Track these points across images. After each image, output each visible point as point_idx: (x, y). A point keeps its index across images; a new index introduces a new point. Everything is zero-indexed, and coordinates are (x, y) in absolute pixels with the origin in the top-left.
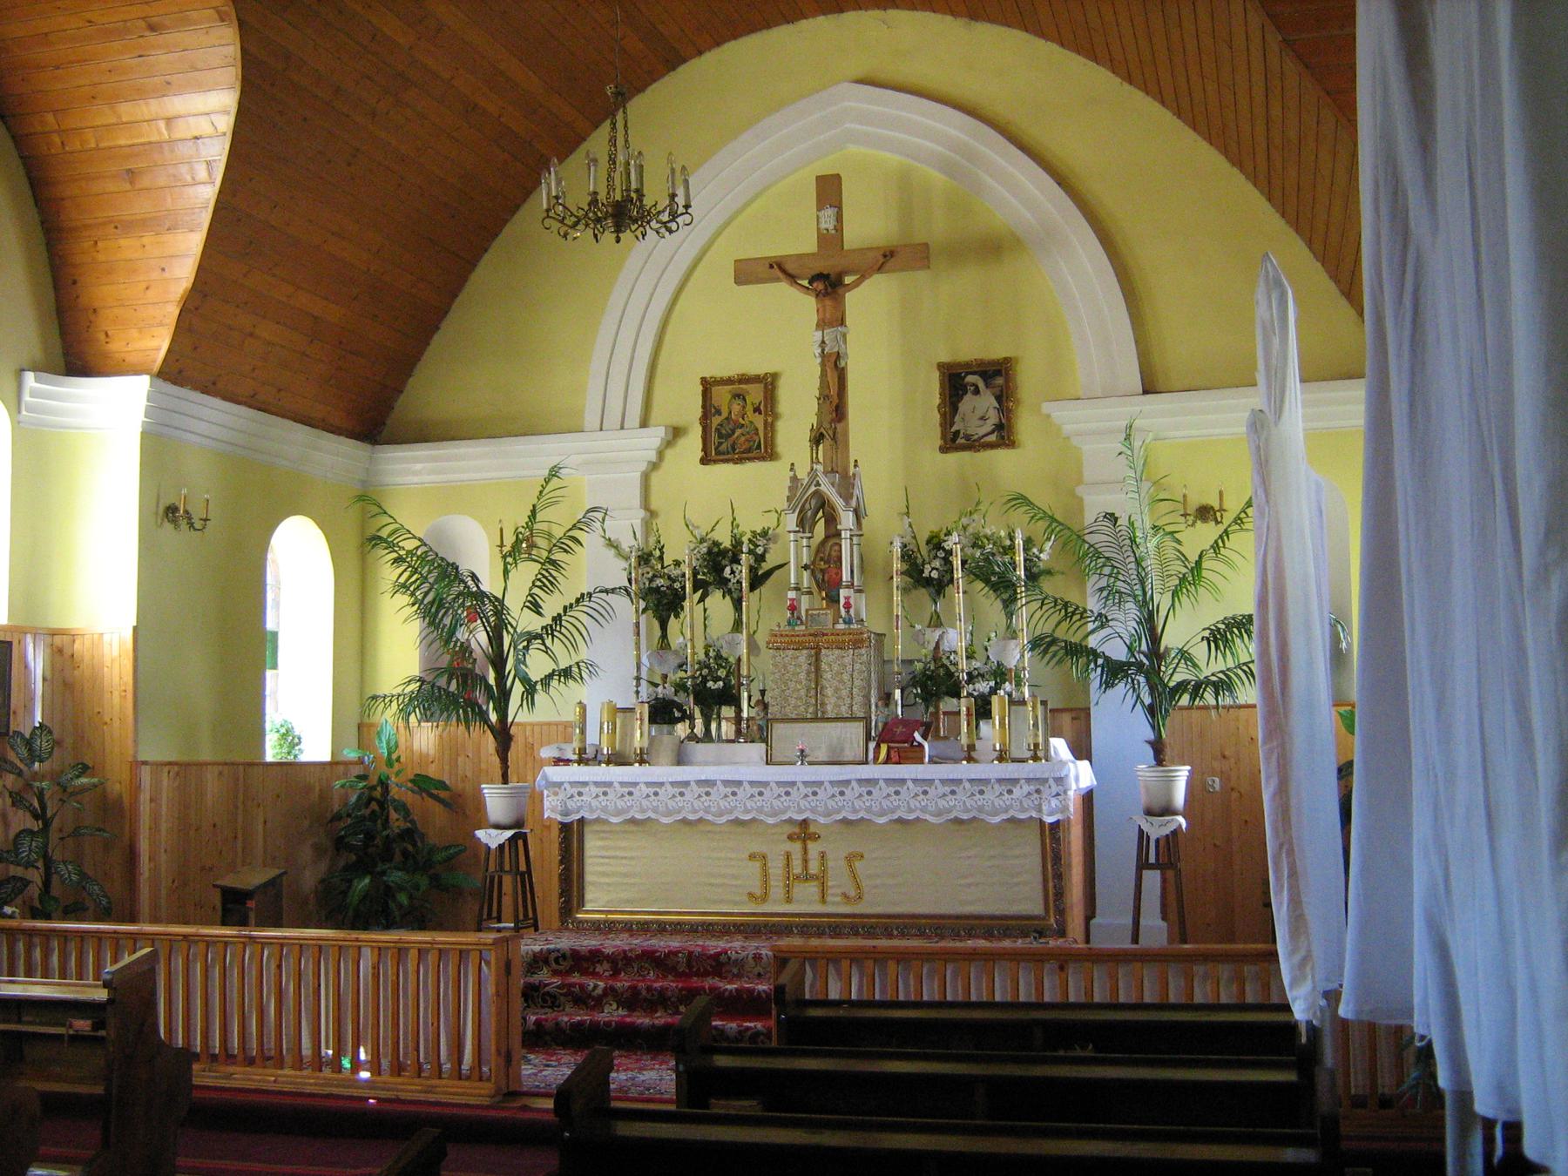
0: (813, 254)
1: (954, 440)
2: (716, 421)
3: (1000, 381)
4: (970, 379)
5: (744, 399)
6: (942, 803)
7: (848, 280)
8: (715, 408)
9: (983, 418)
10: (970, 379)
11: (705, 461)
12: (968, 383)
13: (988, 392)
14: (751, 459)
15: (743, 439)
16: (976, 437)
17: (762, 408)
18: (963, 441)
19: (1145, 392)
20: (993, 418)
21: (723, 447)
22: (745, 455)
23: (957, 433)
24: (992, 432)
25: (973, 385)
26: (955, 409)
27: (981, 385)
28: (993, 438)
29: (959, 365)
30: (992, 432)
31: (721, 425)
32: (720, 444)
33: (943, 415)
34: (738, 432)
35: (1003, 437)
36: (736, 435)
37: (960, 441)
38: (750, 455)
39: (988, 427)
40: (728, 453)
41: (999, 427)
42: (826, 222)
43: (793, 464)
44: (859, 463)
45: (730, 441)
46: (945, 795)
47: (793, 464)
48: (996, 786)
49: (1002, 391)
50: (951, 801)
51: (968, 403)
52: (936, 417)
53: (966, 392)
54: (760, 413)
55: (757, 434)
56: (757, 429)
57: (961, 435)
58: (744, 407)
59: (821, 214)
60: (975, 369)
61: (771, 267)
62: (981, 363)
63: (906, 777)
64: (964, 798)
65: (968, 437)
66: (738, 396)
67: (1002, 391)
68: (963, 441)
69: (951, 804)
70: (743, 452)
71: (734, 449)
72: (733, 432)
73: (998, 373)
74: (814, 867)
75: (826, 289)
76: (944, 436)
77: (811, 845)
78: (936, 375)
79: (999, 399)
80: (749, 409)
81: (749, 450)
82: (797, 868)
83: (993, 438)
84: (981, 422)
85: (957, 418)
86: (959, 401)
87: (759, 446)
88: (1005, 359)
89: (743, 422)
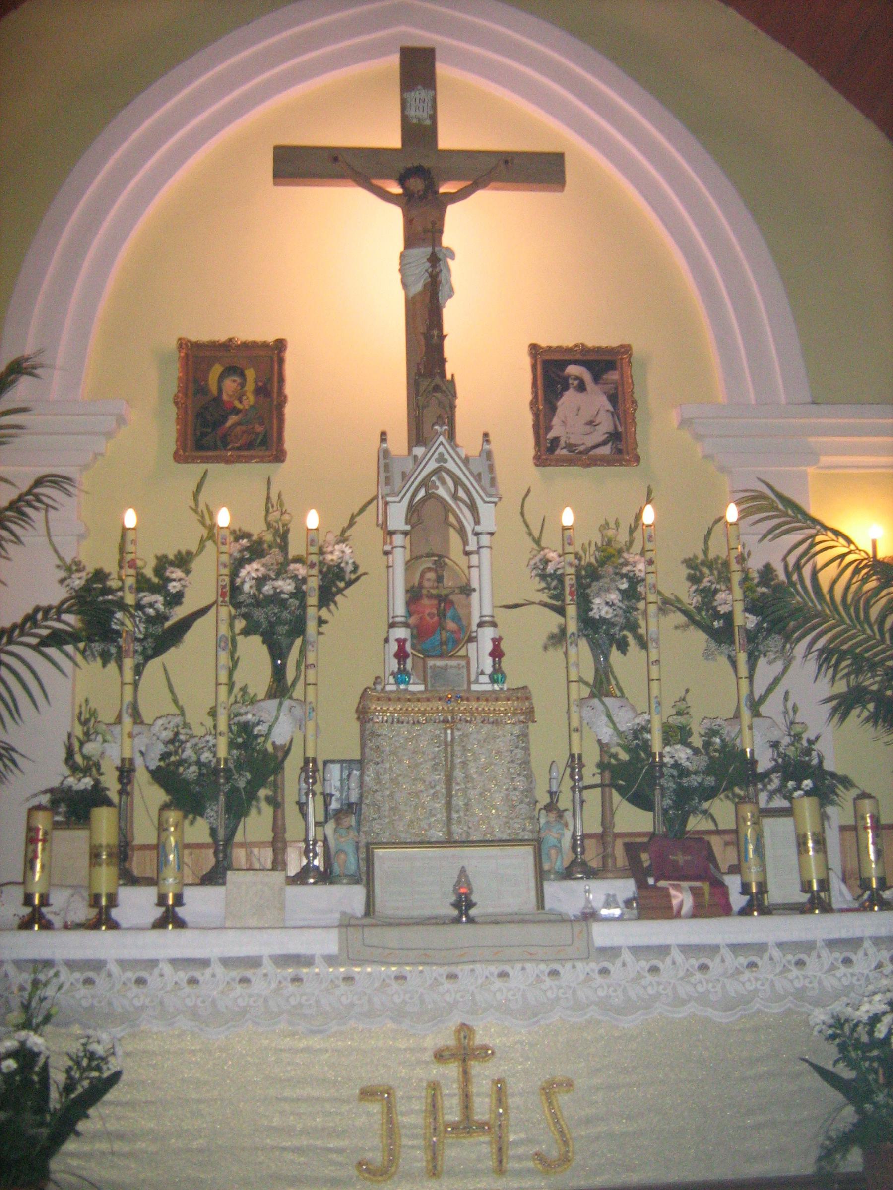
0: (396, 150)
3: (613, 376)
5: (242, 375)
6: (733, 988)
9: (590, 423)
12: (569, 376)
16: (582, 448)
18: (564, 452)
19: (814, 403)
20: (606, 425)
22: (246, 453)
23: (556, 440)
24: (604, 443)
25: (576, 378)
26: (552, 409)
27: (587, 376)
28: (606, 450)
29: (559, 349)
30: (604, 443)
33: (536, 415)
34: (232, 419)
36: (229, 424)
37: (561, 452)
39: (599, 436)
40: (215, 448)
41: (615, 437)
42: (417, 108)
44: (491, 438)
46: (738, 972)
48: (825, 953)
49: (616, 388)
50: (749, 981)
51: (569, 400)
52: (528, 418)
53: (566, 388)
57: (562, 443)
58: (243, 385)
60: (579, 357)
62: (584, 349)
63: (668, 942)
64: (771, 976)
65: (570, 447)
66: (232, 370)
67: (616, 388)
68: (564, 452)
69: (750, 987)
70: (239, 449)
72: (225, 418)
73: (611, 365)
74: (482, 1108)
77: (476, 1068)
78: (526, 361)
79: (613, 398)
80: (250, 386)
81: (249, 446)
82: (452, 1113)
83: (606, 450)
84: (588, 429)
85: (556, 421)
86: (558, 399)
88: (622, 346)
89: (240, 406)
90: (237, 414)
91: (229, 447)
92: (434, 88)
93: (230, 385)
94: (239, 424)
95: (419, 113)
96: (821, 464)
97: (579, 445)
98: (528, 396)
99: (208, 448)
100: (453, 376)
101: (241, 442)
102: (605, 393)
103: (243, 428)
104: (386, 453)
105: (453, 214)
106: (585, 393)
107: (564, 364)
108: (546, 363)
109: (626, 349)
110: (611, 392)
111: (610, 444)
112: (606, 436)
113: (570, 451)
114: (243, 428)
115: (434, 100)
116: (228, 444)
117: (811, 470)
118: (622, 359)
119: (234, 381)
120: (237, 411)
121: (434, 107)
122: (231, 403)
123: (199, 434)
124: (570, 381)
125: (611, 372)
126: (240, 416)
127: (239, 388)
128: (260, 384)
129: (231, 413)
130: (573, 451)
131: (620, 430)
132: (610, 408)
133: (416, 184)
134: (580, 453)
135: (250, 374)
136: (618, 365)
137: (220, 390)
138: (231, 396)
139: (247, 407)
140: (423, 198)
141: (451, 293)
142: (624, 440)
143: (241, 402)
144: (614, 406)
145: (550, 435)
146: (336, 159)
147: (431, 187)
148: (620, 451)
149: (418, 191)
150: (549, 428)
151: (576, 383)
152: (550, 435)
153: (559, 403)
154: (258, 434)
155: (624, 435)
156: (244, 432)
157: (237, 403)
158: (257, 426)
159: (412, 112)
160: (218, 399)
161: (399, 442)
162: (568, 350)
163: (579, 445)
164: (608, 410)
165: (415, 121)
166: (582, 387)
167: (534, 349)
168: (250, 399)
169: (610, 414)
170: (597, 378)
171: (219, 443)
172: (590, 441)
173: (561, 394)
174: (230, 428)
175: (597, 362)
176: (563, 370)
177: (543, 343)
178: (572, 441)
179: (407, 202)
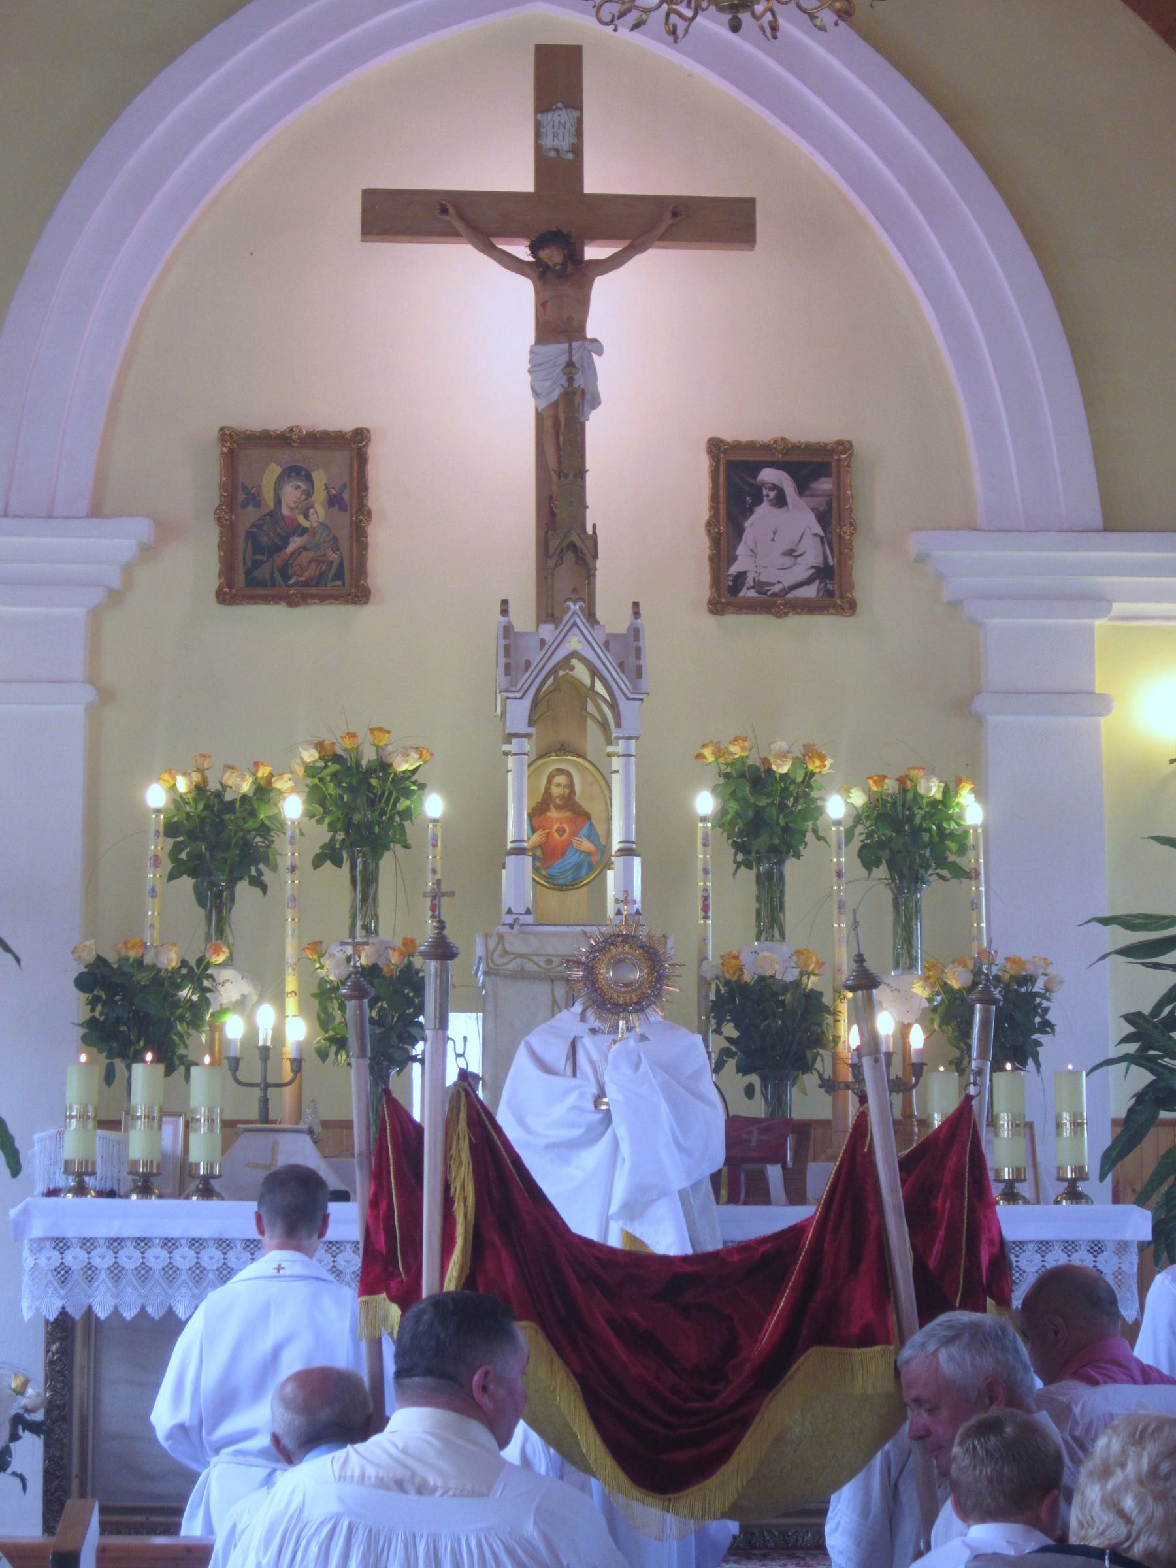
1: (735, 589)
2: (250, 516)
3: (825, 485)
4: (768, 475)
5: (309, 479)
7: (593, 252)
8: (245, 488)
9: (790, 553)
10: (768, 475)
11: (228, 595)
12: (763, 484)
13: (801, 502)
14: (323, 599)
15: (305, 557)
16: (776, 588)
17: (346, 496)
18: (752, 594)
20: (812, 556)
21: (263, 572)
22: (312, 590)
23: (742, 575)
24: (808, 582)
25: (774, 487)
26: (739, 532)
28: (810, 592)
29: (751, 446)
30: (808, 582)
31: (260, 526)
32: (256, 564)
33: (716, 540)
34: (295, 543)
35: (830, 594)
36: (291, 548)
37: (747, 593)
38: (320, 590)
39: (801, 572)
40: (274, 584)
41: (823, 573)
42: (555, 136)
43: (505, 603)
44: (642, 611)
45: (278, 560)
47: (505, 603)
51: (762, 517)
52: (703, 545)
53: (758, 500)
54: (342, 508)
55: (336, 549)
56: (335, 539)
57: (750, 581)
58: (309, 494)
59: (546, 118)
60: (779, 457)
61: (444, 211)
65: (760, 586)
66: (294, 472)
67: (829, 503)
68: (752, 594)
71: (286, 577)
72: (286, 544)
75: (564, 264)
76: (716, 582)
78: (703, 463)
79: (823, 518)
80: (319, 497)
83: (810, 592)
84: (788, 561)
85: (741, 550)
86: (746, 518)
87: (339, 575)
88: (839, 443)
89: (305, 524)
90: (301, 535)
91: (291, 582)
92: (579, 108)
93: (291, 493)
94: (305, 548)
95: (558, 143)
96: (1112, 614)
97: (773, 584)
98: (703, 512)
99: (263, 584)
100: (594, 526)
101: (307, 574)
102: (813, 510)
103: (310, 554)
104: (507, 630)
105: (602, 289)
106: (784, 509)
107: (754, 468)
108: (731, 466)
109: (844, 447)
110: (822, 508)
111: (817, 583)
112: (813, 571)
113: (760, 593)
114: (310, 554)
115: (580, 122)
116: (290, 578)
117: (1098, 623)
118: (839, 460)
119: (298, 487)
120: (304, 531)
121: (579, 134)
122: (294, 520)
123: (249, 563)
124: (765, 492)
125: (823, 479)
126: (306, 537)
127: (304, 497)
128: (333, 492)
129: (294, 533)
130: (765, 594)
131: (831, 563)
132: (821, 533)
133: (552, 255)
134: (774, 595)
135: (320, 478)
136: (834, 470)
137: (278, 502)
138: (292, 509)
139: (315, 525)
140: (562, 275)
141: (596, 402)
142: (837, 577)
143: (306, 517)
144: (824, 529)
145: (733, 570)
146: (444, 211)
147: (574, 257)
148: (830, 594)
149: (555, 265)
150: (732, 559)
151: (772, 494)
152: (733, 570)
153: (747, 524)
154: (332, 562)
155: (836, 571)
156: (313, 560)
157: (301, 519)
158: (329, 552)
159: (548, 142)
160: (274, 515)
161: (524, 617)
162: (766, 447)
163: (773, 584)
164: (816, 535)
165: (552, 154)
166: (780, 501)
167: (715, 447)
168: (320, 511)
169: (818, 540)
170: (802, 488)
171: (277, 575)
172: (789, 579)
173: (752, 512)
174: (292, 554)
175: (804, 464)
176: (755, 477)
177: (728, 436)
178: (763, 579)
179: (539, 272)
